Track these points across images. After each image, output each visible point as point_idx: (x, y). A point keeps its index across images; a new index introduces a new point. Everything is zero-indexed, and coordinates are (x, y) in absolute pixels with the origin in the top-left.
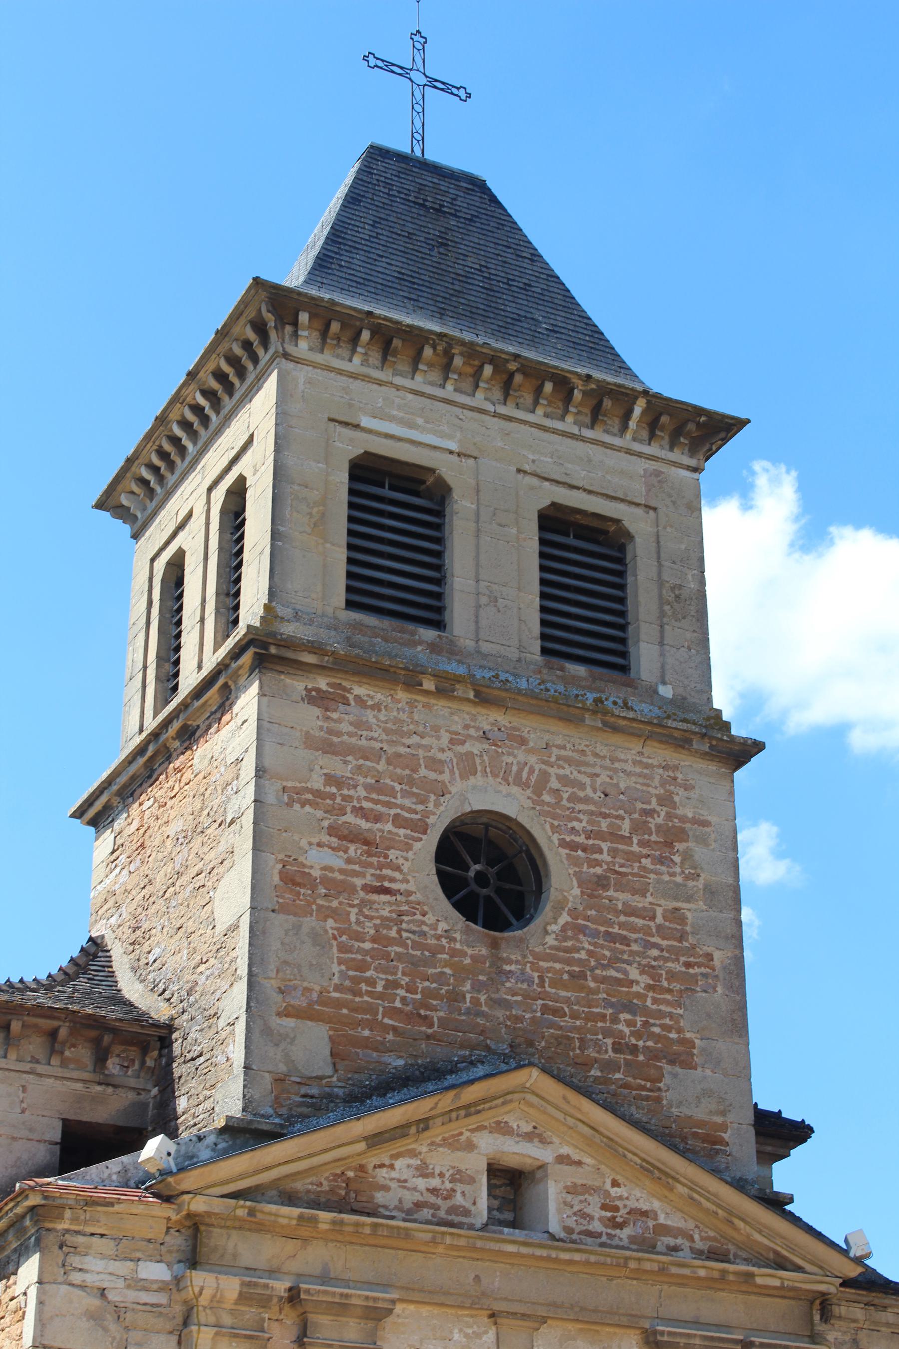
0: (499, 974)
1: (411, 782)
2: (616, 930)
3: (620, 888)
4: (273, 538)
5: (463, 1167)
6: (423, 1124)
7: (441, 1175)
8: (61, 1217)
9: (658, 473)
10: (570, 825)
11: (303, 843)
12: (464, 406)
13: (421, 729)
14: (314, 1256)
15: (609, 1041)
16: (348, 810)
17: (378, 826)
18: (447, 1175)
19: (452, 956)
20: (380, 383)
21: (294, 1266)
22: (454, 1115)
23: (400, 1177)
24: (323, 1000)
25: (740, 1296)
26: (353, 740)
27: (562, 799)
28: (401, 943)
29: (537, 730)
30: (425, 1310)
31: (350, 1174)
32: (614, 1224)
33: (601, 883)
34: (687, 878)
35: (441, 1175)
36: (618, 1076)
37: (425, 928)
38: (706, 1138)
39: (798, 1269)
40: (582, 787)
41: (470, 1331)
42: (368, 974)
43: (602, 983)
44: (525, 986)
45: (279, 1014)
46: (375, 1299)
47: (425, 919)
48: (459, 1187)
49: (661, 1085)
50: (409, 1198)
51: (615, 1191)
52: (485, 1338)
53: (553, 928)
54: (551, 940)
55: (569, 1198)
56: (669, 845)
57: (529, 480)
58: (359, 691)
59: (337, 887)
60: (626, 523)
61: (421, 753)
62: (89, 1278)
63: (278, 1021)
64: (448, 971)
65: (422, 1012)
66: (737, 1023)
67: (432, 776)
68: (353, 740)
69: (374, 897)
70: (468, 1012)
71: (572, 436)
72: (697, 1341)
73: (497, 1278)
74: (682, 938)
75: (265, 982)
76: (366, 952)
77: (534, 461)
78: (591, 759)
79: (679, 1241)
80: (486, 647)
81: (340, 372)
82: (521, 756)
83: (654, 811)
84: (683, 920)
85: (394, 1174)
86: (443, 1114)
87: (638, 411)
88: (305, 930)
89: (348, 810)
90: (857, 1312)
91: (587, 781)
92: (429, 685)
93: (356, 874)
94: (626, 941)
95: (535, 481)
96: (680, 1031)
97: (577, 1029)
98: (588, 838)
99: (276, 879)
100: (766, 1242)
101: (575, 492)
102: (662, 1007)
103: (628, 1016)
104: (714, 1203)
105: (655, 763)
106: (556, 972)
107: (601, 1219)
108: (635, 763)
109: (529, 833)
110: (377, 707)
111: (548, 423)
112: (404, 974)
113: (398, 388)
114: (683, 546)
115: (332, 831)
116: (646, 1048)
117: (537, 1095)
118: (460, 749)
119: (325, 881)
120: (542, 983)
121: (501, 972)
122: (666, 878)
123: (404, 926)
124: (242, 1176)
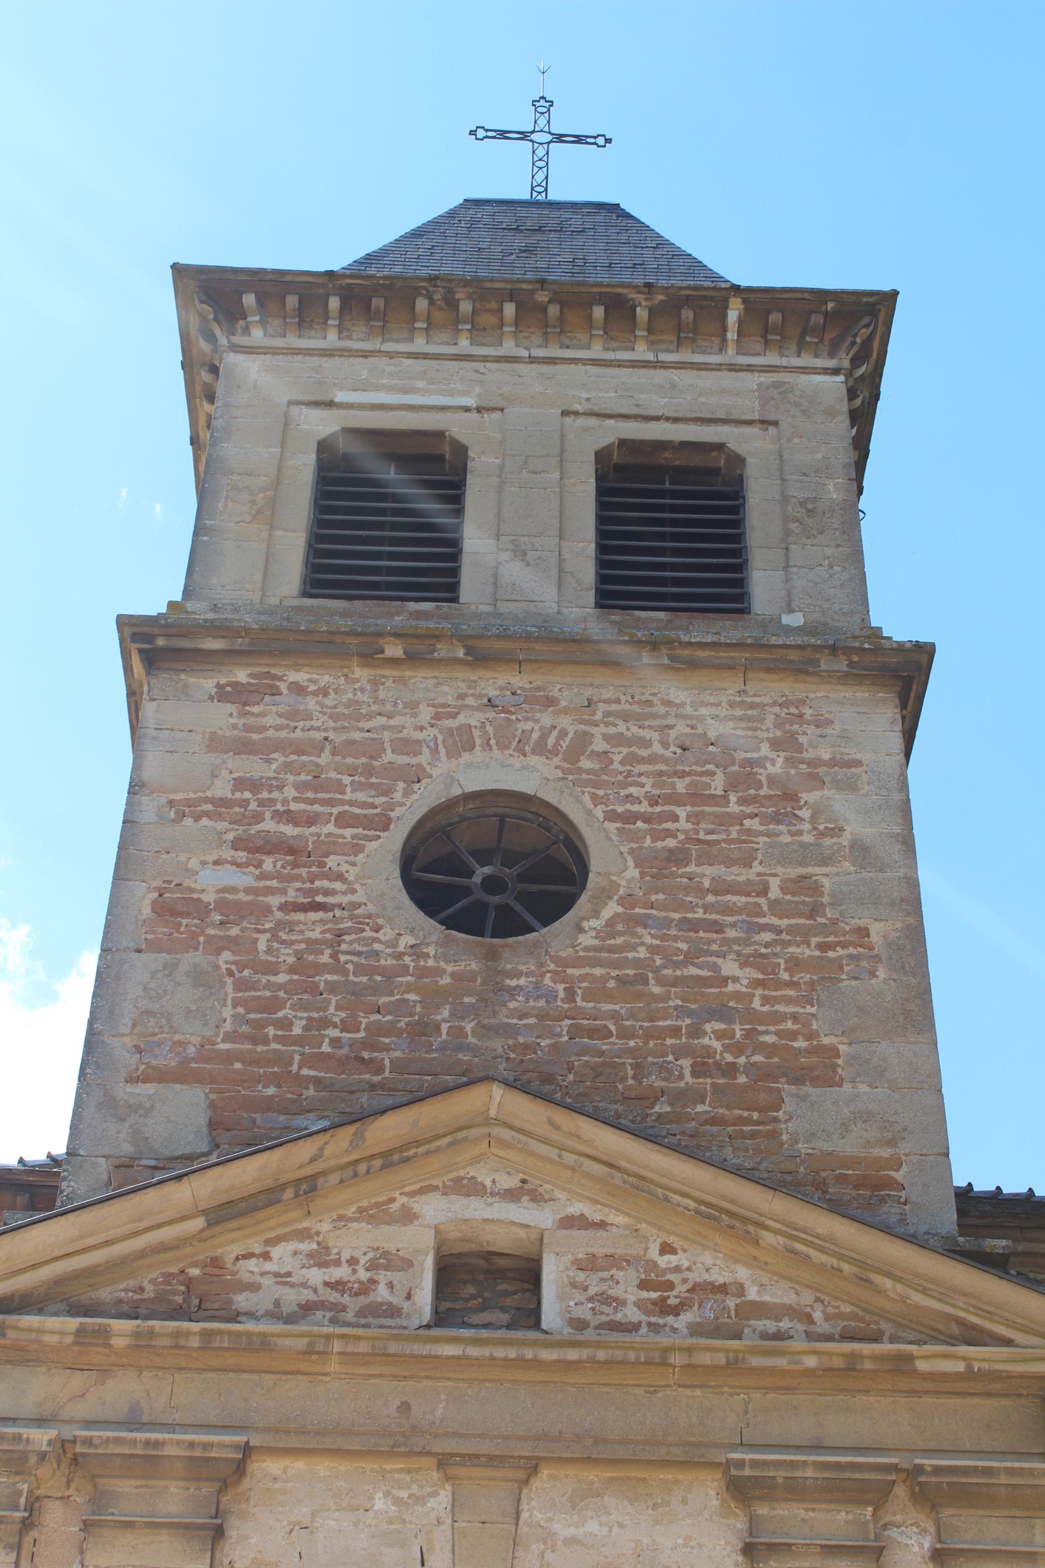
0: (496, 989)
1: (369, 771)
2: (700, 914)
3: (706, 859)
4: (196, 533)
5: (392, 1249)
6: (308, 1187)
7: (353, 1262)
9: (777, 385)
10: (623, 793)
11: (194, 863)
12: (485, 359)
13: (389, 708)
15: (686, 1063)
16: (268, 815)
17: (314, 829)
18: (363, 1260)
19: (419, 978)
20: (365, 354)
21: (80, 1410)
22: (362, 1167)
23: (276, 1266)
26: (283, 734)
27: (612, 762)
28: (338, 968)
30: (323, 1467)
31: (195, 1272)
32: (663, 1308)
33: (677, 857)
34: (822, 835)
36: (700, 1108)
37: (377, 946)
39: (1008, 1342)
40: (646, 743)
41: (404, 1494)
42: (280, 1014)
43: (673, 986)
44: (542, 1003)
45: (130, 1080)
46: (205, 1446)
47: (380, 935)
48: (382, 1277)
49: (780, 1114)
50: (291, 1298)
51: (665, 1261)
52: (431, 1503)
53: (594, 923)
54: (586, 940)
55: (581, 1276)
57: (581, 421)
58: (293, 676)
59: (232, 909)
60: (732, 445)
61: (387, 735)
63: (129, 1088)
64: (412, 997)
65: (366, 1055)
66: (916, 1013)
67: (403, 760)
68: (283, 734)
69: (300, 916)
70: (443, 1047)
71: (645, 364)
72: (810, 1473)
73: (438, 1405)
74: (814, 911)
75: (116, 1042)
76: (280, 987)
77: (588, 400)
78: (661, 709)
79: (785, 1324)
80: (503, 607)
81: (309, 352)
82: (546, 719)
83: (766, 758)
84: (816, 889)
85: (269, 1266)
86: (342, 1168)
88: (183, 967)
89: (268, 815)
91: (655, 736)
92: (394, 650)
93: (271, 891)
94: (717, 927)
95: (592, 421)
96: (810, 1036)
97: (631, 1052)
98: (654, 803)
99: (147, 911)
100: (935, 1305)
102: (780, 1008)
103: (720, 1026)
104: (834, 1254)
105: (766, 700)
106: (594, 979)
107: (638, 1304)
110: (324, 692)
111: (610, 356)
112: (338, 1008)
113: (390, 355)
114: (820, 456)
117: (512, 1128)
118: (449, 723)
119: (221, 905)
120: (570, 994)
121: (502, 989)
122: (786, 839)
123: (344, 947)
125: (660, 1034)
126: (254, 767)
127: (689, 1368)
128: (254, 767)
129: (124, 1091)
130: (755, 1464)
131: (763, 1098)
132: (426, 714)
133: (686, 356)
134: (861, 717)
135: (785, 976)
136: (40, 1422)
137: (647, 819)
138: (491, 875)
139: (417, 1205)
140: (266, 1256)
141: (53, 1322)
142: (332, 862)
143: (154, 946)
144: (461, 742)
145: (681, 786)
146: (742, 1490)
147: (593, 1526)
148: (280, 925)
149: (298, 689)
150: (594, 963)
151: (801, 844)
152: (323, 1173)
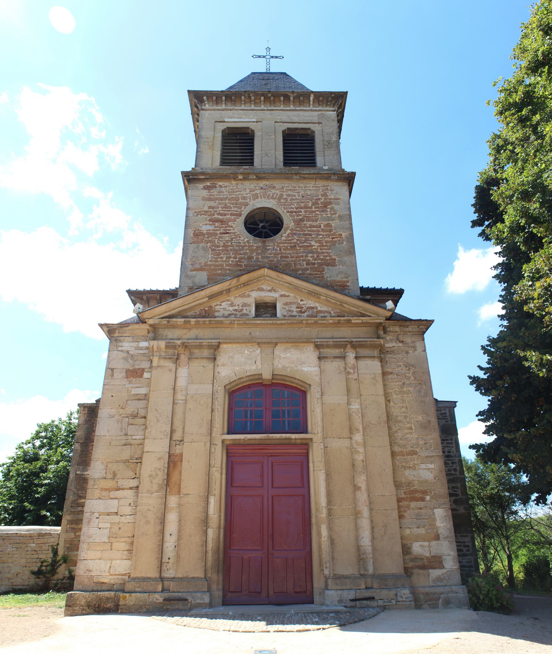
0: (265, 249)
1: (237, 204)
2: (307, 232)
4: (197, 152)
5: (246, 302)
6: (228, 291)
7: (238, 305)
8: (115, 333)
11: (201, 225)
12: (257, 110)
14: (194, 333)
15: (305, 263)
20: (231, 110)
21: (186, 337)
23: (223, 307)
24: (206, 265)
25: (349, 328)
26: (218, 196)
28: (232, 246)
29: (278, 184)
30: (235, 346)
31: (207, 309)
32: (301, 312)
33: (302, 220)
34: (332, 215)
35: (238, 305)
38: (340, 286)
40: (295, 196)
45: (191, 271)
46: (211, 342)
48: (244, 308)
50: (226, 313)
51: (301, 303)
53: (285, 235)
54: (283, 238)
55: (284, 306)
56: (326, 207)
57: (279, 124)
58: (219, 184)
59: (209, 234)
61: (240, 196)
62: (124, 348)
64: (248, 251)
66: (351, 251)
67: (244, 201)
69: (224, 235)
70: (255, 261)
72: (331, 343)
73: (257, 333)
74: (330, 231)
75: (187, 263)
76: (221, 250)
78: (298, 188)
79: (326, 314)
80: (263, 167)
81: (218, 110)
82: (274, 191)
84: (331, 226)
85: (221, 307)
87: (312, 98)
88: (200, 247)
90: (397, 329)
91: (297, 194)
92: (240, 177)
93: (217, 230)
94: (311, 235)
95: (281, 124)
96: (330, 256)
97: (293, 261)
99: (192, 235)
100: (356, 309)
101: (295, 124)
102: (324, 251)
103: (311, 255)
106: (285, 246)
107: (296, 311)
108: (313, 187)
109: (278, 213)
113: (236, 110)
115: (210, 220)
116: (318, 263)
118: (253, 193)
119: (207, 234)
120: (280, 250)
121: (266, 249)
122: (325, 216)
124: (165, 312)
125: (299, 257)
126: (212, 204)
127: (307, 323)
128: (212, 204)
129: (190, 273)
130: (320, 342)
131: (321, 269)
132: (248, 191)
133: (301, 108)
134: (340, 189)
135: (325, 244)
136: (178, 339)
137: (295, 212)
138: (263, 225)
139: (251, 293)
140: (221, 305)
141: (179, 320)
142: (230, 223)
143: (194, 243)
144: (256, 197)
145: (302, 205)
146: (318, 347)
147: (288, 355)
148: (220, 237)
149: (221, 186)
150: (285, 243)
151: (328, 217)
152: (232, 288)
